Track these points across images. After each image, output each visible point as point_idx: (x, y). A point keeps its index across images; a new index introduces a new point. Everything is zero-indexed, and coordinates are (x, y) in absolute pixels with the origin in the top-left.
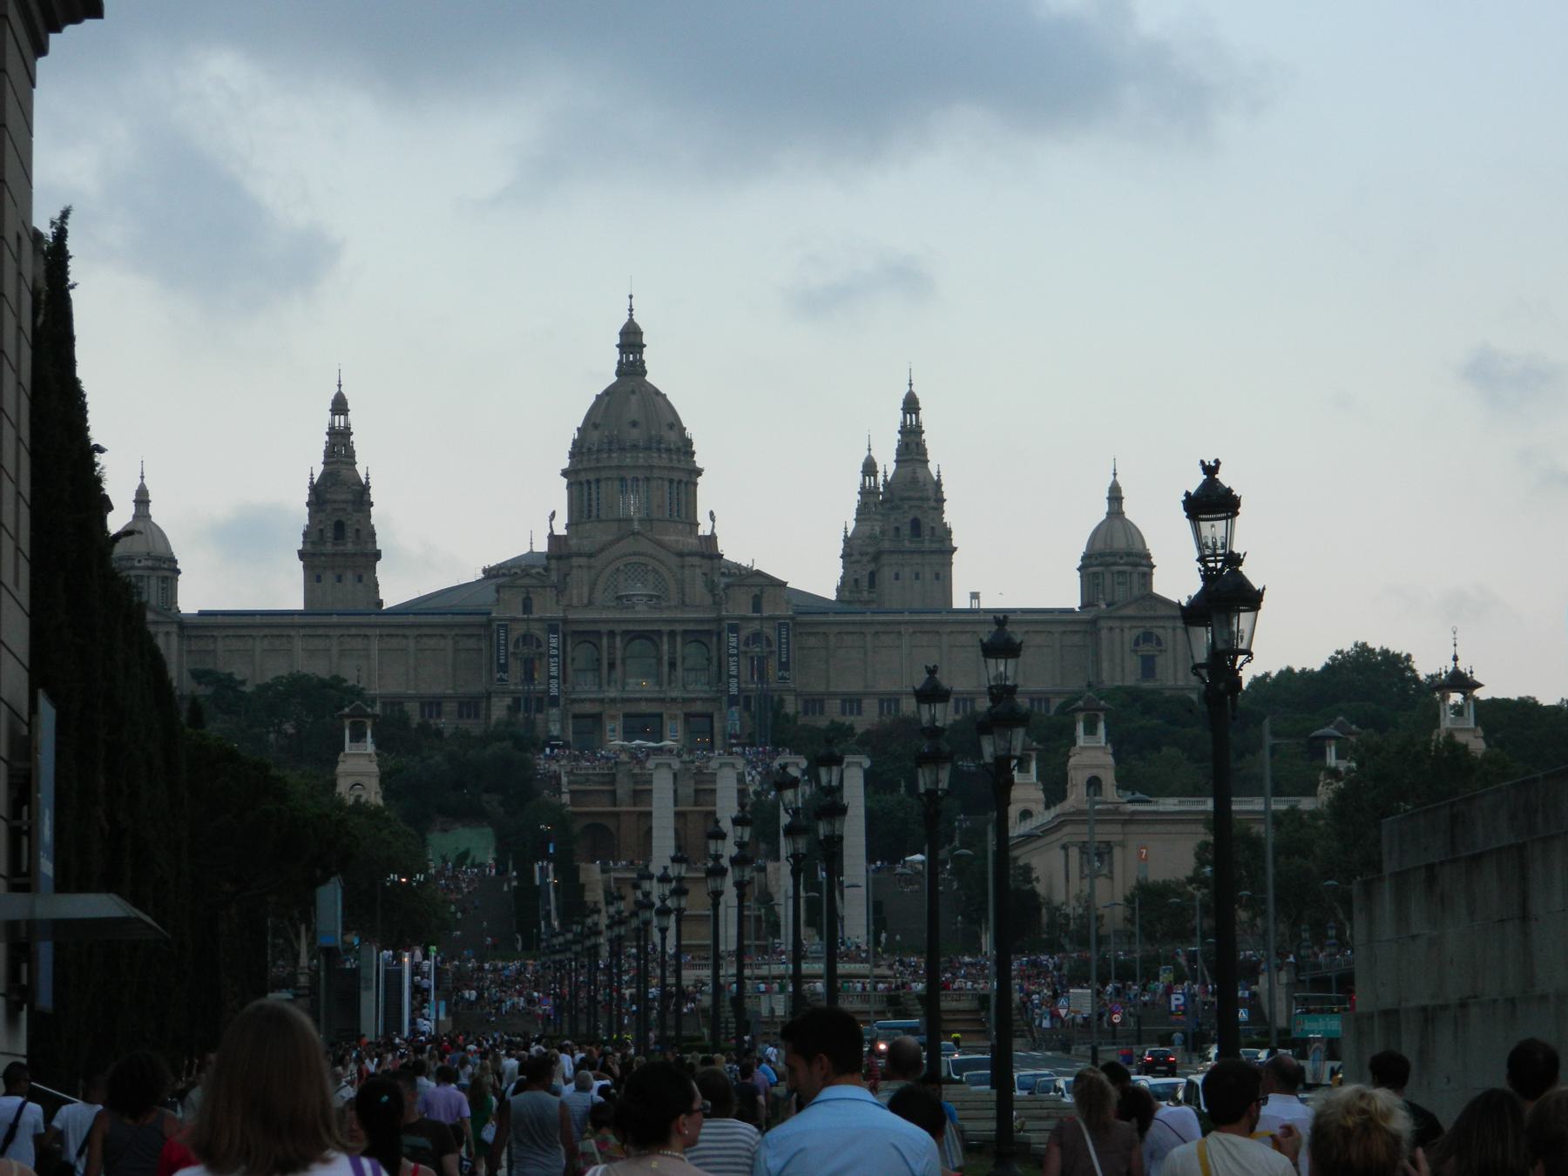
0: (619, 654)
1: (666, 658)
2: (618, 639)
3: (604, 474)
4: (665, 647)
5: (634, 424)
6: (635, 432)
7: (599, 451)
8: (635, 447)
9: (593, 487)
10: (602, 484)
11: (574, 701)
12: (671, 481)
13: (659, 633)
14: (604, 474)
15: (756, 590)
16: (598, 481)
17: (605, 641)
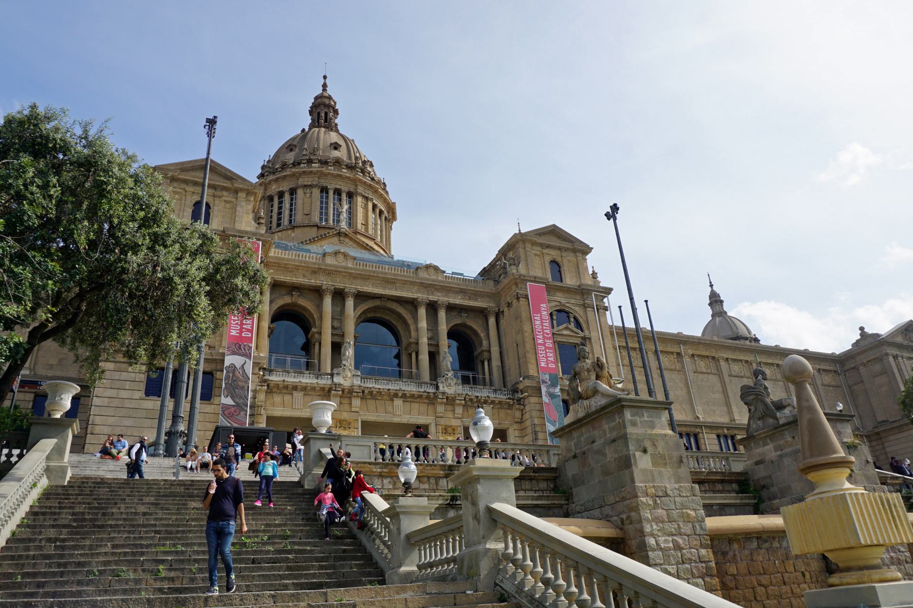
0: (350, 327)
1: (424, 341)
2: (350, 303)
3: (303, 181)
4: (423, 324)
5: (336, 147)
6: (336, 154)
7: (296, 164)
8: (338, 162)
9: (287, 197)
10: (300, 192)
11: (271, 389)
12: (374, 206)
13: (412, 304)
14: (303, 181)
15: (554, 254)
16: (293, 192)
17: (328, 301)
